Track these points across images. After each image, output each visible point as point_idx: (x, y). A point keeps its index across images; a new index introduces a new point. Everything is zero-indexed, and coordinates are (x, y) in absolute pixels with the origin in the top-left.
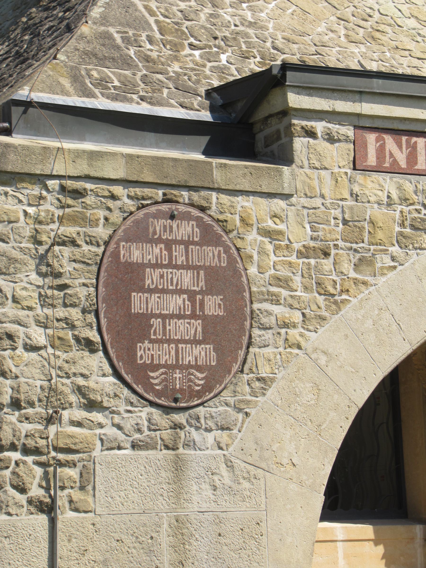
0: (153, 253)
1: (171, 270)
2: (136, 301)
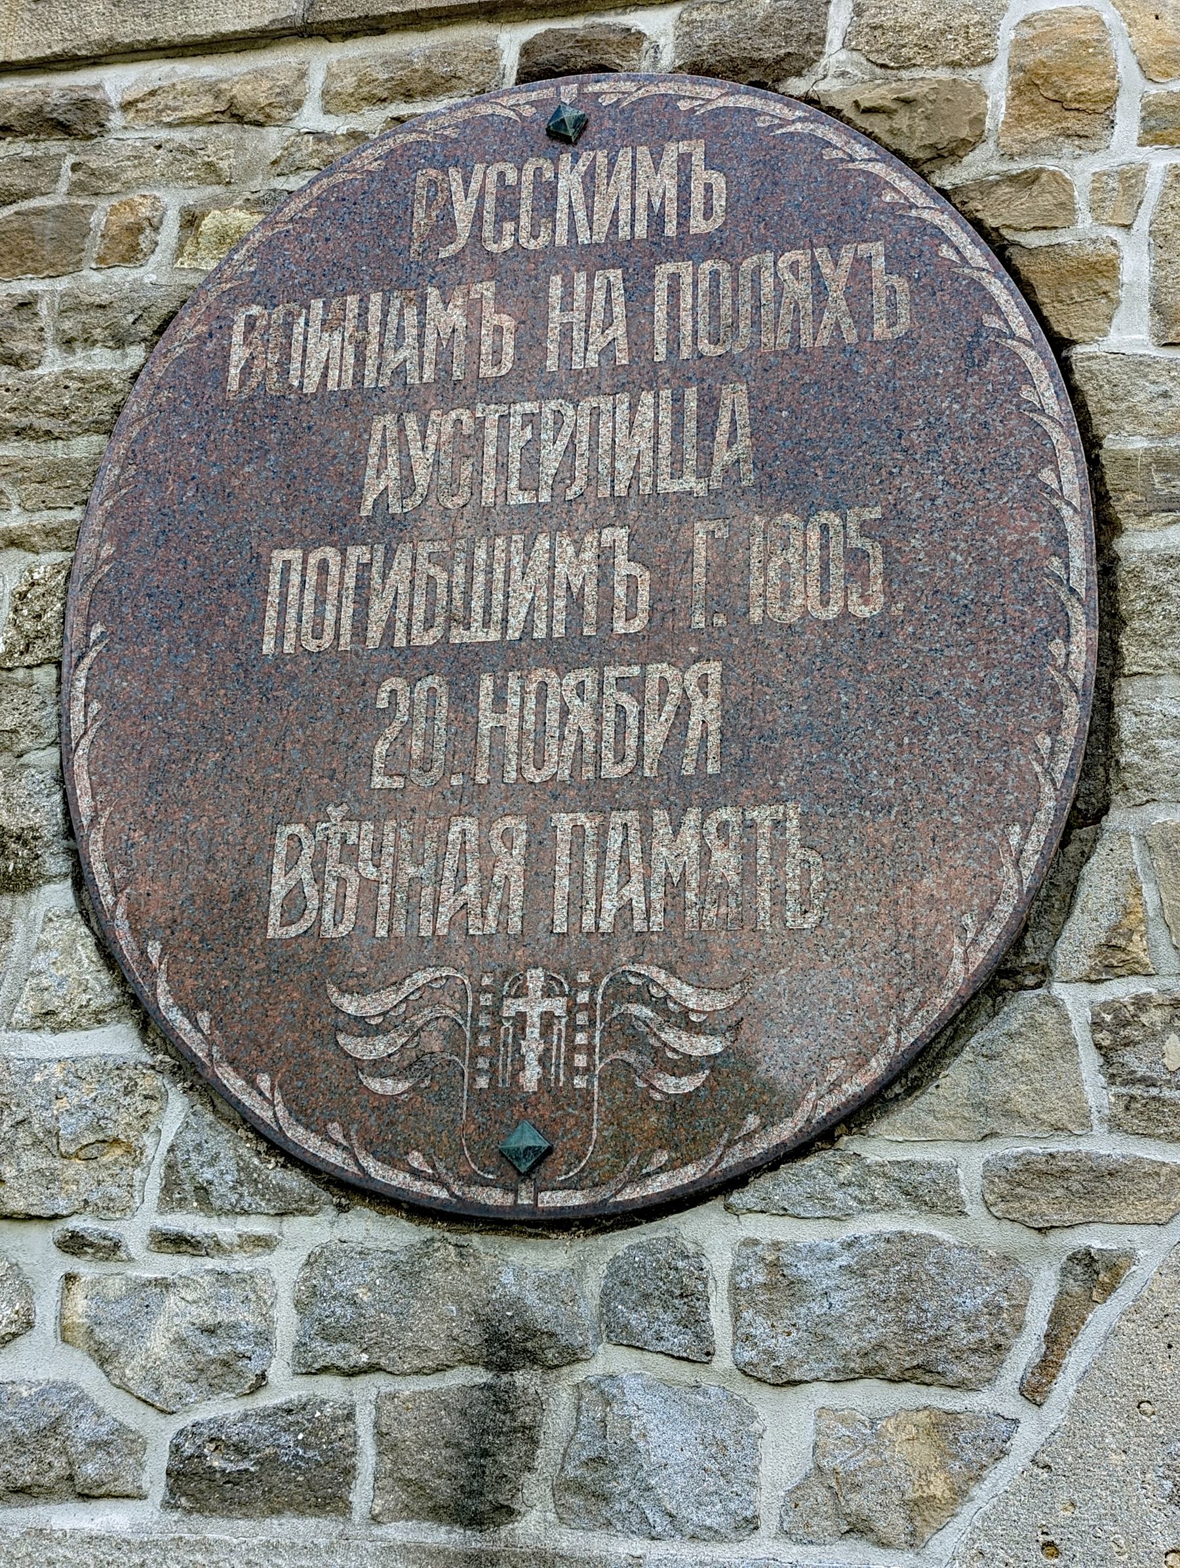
0: (421, 336)
2: (294, 591)
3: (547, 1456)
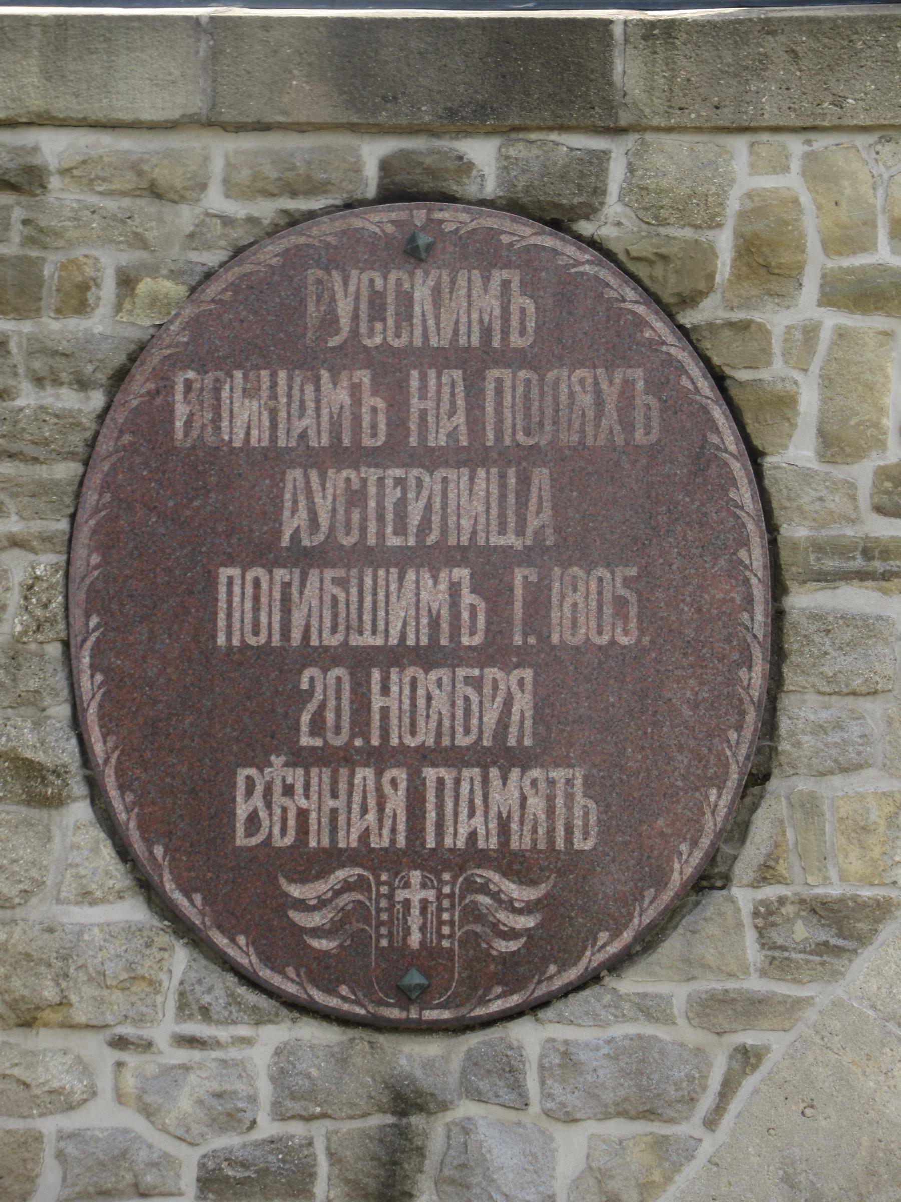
0: (318, 409)
1: (399, 472)
2: (236, 600)
3: (431, 1164)
